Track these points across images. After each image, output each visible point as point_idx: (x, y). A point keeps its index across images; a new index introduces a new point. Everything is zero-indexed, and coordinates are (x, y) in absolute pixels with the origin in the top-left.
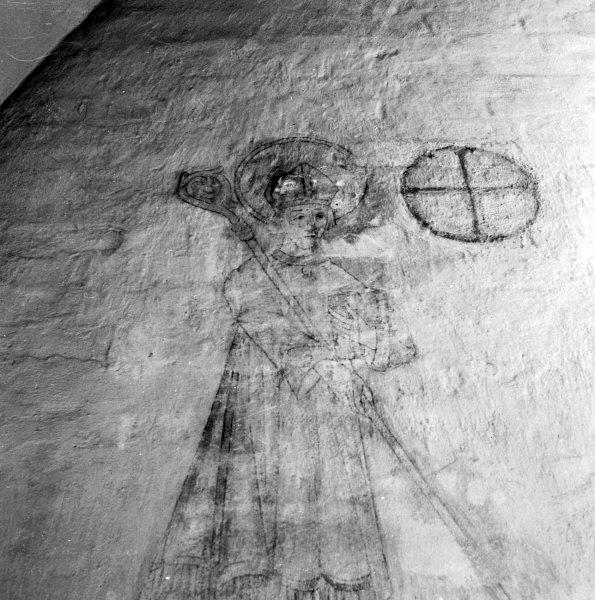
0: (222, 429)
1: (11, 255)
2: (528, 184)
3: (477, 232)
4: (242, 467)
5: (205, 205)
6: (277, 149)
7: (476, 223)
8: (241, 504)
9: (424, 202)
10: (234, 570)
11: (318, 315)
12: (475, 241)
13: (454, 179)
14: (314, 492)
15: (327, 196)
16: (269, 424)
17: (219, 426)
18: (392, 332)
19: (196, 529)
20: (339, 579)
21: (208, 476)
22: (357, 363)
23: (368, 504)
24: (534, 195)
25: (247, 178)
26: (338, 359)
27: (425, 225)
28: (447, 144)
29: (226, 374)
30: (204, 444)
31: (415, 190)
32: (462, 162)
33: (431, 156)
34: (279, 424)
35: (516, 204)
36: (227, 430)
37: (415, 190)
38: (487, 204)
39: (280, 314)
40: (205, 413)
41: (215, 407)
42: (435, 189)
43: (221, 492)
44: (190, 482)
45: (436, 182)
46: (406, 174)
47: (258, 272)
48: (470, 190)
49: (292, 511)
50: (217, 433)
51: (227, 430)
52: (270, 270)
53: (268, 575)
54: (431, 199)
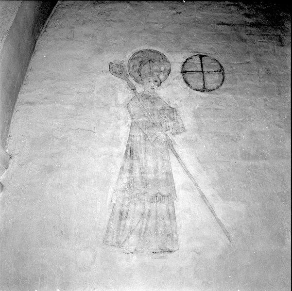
0: (130, 153)
1: (59, 93)
2: (221, 70)
3: (204, 88)
4: (136, 163)
5: (119, 76)
6: (139, 55)
7: (204, 85)
8: (137, 173)
9: (189, 77)
10: (137, 192)
11: (156, 117)
12: (204, 91)
13: (199, 69)
14: (156, 172)
15: (157, 74)
16: (143, 151)
17: (129, 151)
18: (178, 122)
19: (126, 181)
20: (165, 193)
21: (127, 166)
22: (168, 132)
23: (169, 174)
24: (223, 75)
25: (131, 65)
26: (162, 131)
27: (189, 85)
28: (198, 54)
29: (130, 135)
30: (126, 157)
31: (185, 72)
32: (201, 61)
33: (191, 58)
34: (146, 151)
35: (217, 77)
36: (131, 152)
37: (185, 72)
38: (208, 78)
39: (145, 116)
40: (125, 148)
41: (128, 146)
42: (192, 71)
43: (131, 171)
44: (122, 168)
45: (192, 69)
46: (183, 65)
47: (137, 101)
48: (203, 72)
49: (151, 176)
50: (129, 154)
51: (131, 152)
52: (141, 100)
53: (145, 193)
54: (191, 75)
